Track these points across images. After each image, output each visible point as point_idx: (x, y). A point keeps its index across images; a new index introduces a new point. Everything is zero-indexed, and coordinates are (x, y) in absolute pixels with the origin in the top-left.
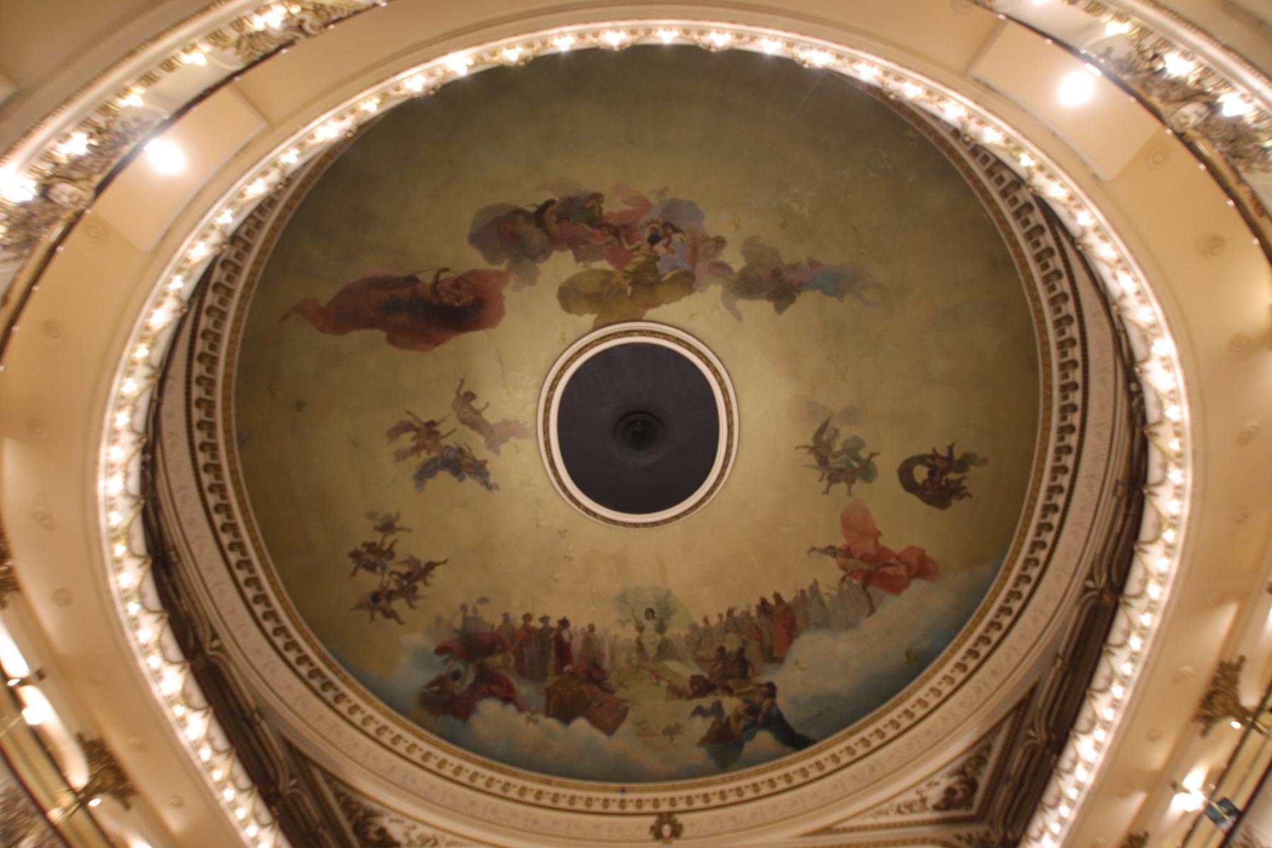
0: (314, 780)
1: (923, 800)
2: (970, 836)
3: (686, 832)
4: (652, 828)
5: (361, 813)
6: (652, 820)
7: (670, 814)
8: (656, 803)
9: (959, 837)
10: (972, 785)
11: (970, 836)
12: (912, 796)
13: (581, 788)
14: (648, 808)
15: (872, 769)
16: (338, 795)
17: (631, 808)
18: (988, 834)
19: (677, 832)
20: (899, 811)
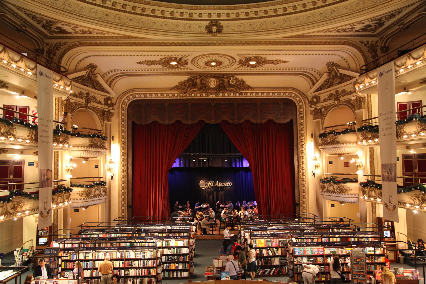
0: (10, 9)
1: (352, 28)
2: (368, 42)
3: (225, 30)
4: (207, 27)
5: (44, 21)
6: (207, 23)
7: (217, 21)
8: (210, 15)
9: (362, 42)
10: (382, 24)
11: (368, 42)
12: (349, 27)
13: (167, 7)
14: (205, 17)
15: (333, 12)
16: (28, 15)
17: (196, 17)
18: (377, 42)
19: (220, 30)
20: (338, 31)
